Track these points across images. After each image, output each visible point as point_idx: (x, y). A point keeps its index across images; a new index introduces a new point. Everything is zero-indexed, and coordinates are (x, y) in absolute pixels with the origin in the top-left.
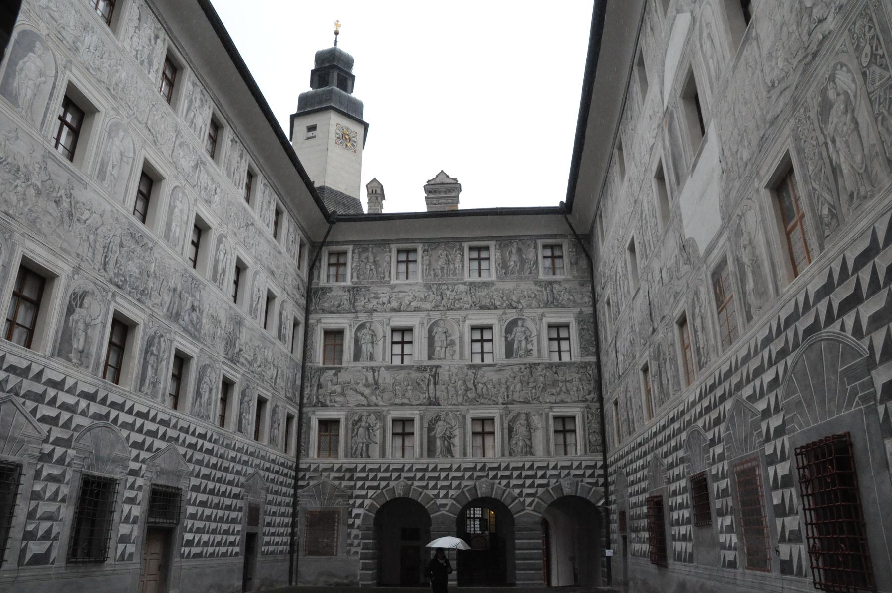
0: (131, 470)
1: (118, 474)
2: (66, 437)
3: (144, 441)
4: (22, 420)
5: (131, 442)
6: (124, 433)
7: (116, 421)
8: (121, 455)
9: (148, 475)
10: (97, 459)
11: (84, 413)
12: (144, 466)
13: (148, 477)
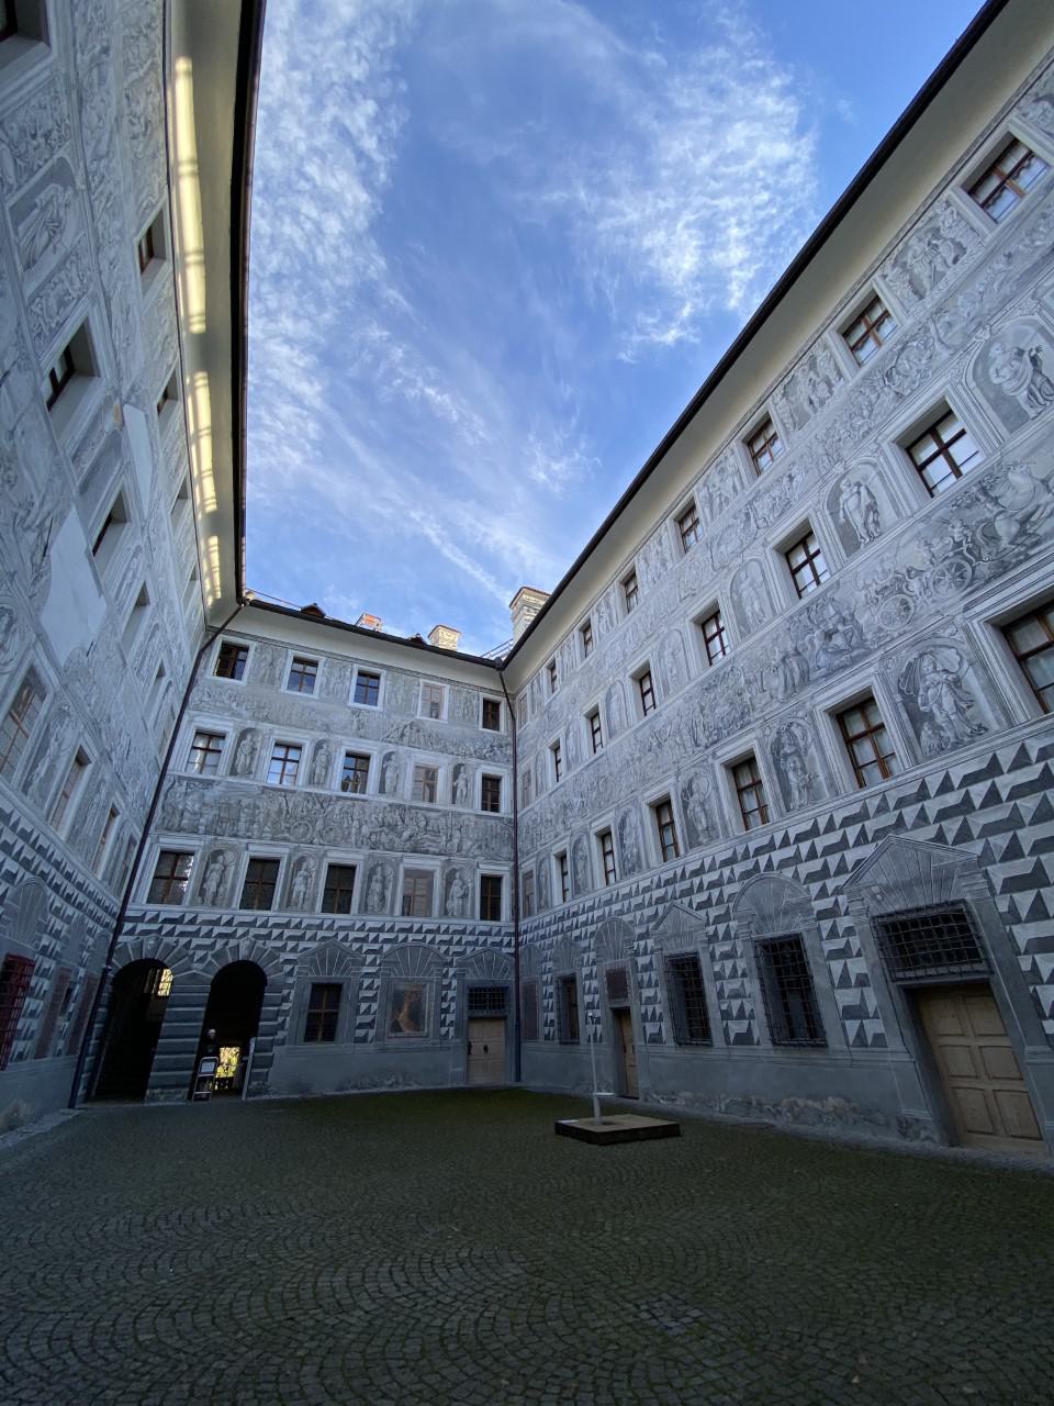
0: (819, 912)
1: (798, 925)
2: (723, 912)
3: (825, 866)
4: (686, 915)
5: (802, 877)
6: (788, 873)
7: (769, 866)
8: (794, 900)
9: (858, 906)
10: (763, 918)
11: (731, 881)
12: (841, 898)
13: (859, 911)
